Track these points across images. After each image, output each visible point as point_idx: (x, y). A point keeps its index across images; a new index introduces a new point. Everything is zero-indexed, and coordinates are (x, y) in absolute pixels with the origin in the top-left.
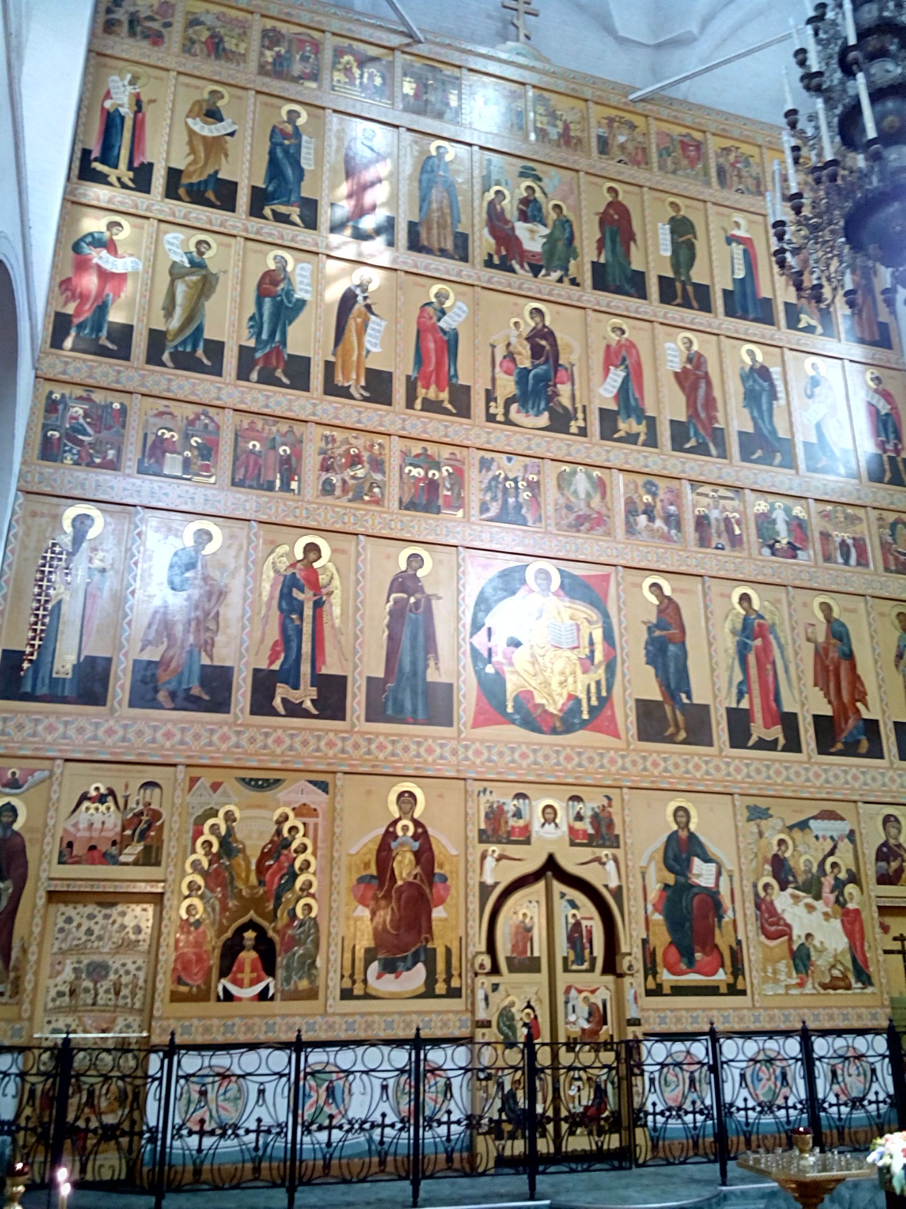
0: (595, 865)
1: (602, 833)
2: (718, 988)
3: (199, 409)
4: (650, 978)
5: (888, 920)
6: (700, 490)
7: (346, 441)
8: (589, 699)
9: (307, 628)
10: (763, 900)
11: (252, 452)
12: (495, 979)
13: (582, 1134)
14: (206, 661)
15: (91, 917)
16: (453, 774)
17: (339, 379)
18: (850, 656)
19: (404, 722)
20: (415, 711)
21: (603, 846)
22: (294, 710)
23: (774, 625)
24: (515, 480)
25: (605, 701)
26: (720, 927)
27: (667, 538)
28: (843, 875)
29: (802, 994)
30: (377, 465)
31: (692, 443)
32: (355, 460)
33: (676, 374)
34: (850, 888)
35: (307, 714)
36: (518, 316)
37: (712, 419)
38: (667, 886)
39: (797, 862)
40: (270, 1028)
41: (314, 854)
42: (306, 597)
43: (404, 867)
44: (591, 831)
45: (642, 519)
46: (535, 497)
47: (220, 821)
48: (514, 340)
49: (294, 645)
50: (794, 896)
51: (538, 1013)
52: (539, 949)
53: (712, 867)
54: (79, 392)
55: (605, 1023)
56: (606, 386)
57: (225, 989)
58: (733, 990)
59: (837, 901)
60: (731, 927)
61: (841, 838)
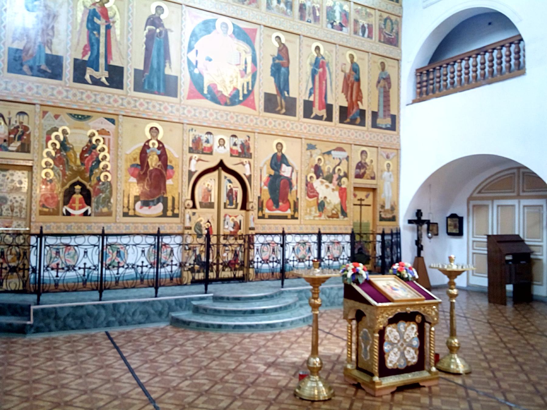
0: (241, 165)
1: (245, 152)
5: (357, 193)
8: (243, 90)
9: (102, 40)
12: (194, 210)
16: (177, 121)
18: (358, 80)
20: (159, 87)
21: (245, 157)
22: (96, 82)
23: (328, 63)
25: (250, 92)
27: (285, 13)
28: (342, 174)
34: (344, 179)
35: (103, 85)
38: (270, 175)
41: (109, 152)
42: (101, 22)
43: (153, 161)
44: (240, 151)
47: (60, 133)
49: (95, 47)
50: (322, 182)
51: (212, 224)
52: (214, 199)
53: (290, 169)
55: (240, 229)
57: (66, 210)
58: (293, 217)
59: (338, 184)
61: (343, 159)
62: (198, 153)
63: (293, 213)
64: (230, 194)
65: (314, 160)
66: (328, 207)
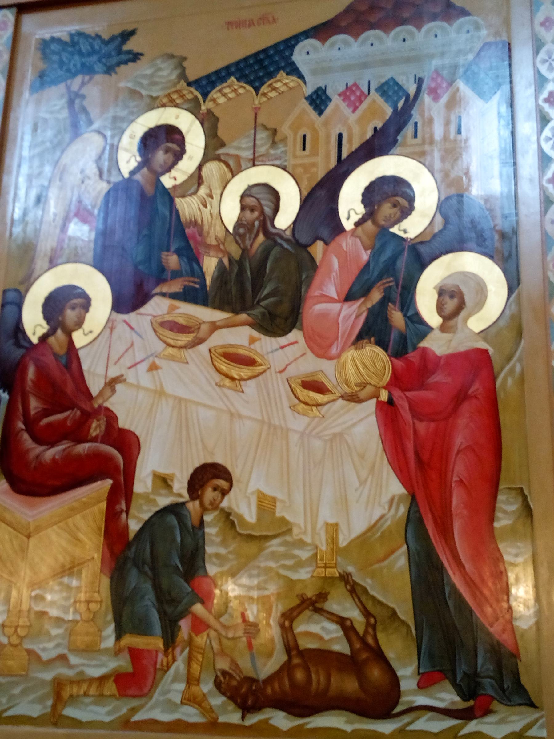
29: (126, 724)
66: (240, 593)
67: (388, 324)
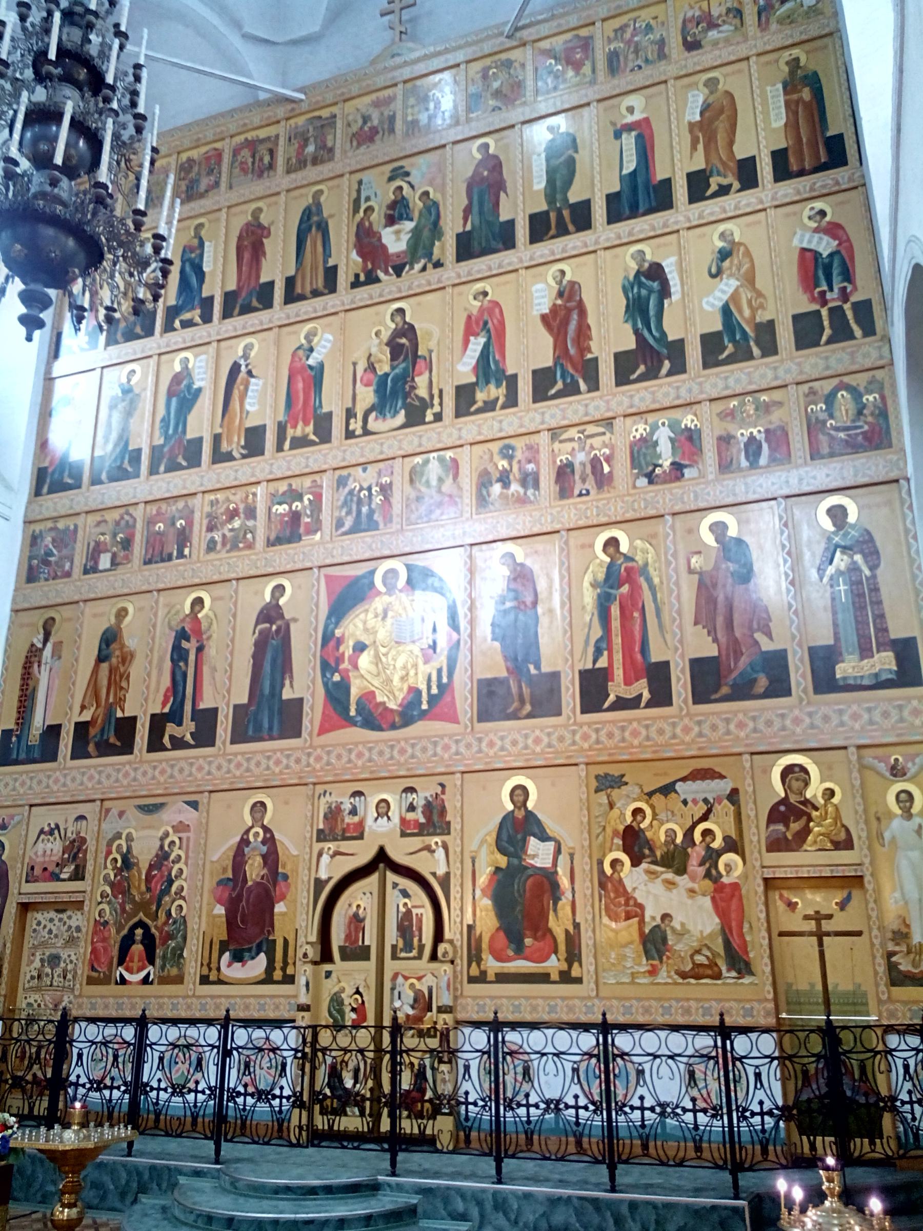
0: (425, 853)
1: (434, 820)
2: (548, 975)
3: (122, 510)
4: (474, 964)
6: (564, 437)
7: (228, 500)
8: (429, 688)
10: (609, 878)
11: (159, 533)
12: (327, 967)
13: (354, 1115)
14: (119, 714)
15: (51, 920)
17: (225, 447)
19: (261, 739)
20: (271, 728)
22: (178, 744)
24: (369, 489)
26: (555, 910)
27: (522, 501)
28: (717, 844)
29: (653, 984)
30: (251, 513)
31: (559, 385)
32: (233, 514)
33: (544, 318)
35: (187, 746)
36: (380, 324)
37: (583, 349)
38: (498, 869)
39: (657, 833)
40: (553, 1009)
41: (186, 864)
42: (190, 646)
43: (254, 870)
44: (422, 820)
45: (497, 488)
46: (387, 499)
47: (123, 842)
48: (374, 350)
50: (648, 872)
52: (370, 938)
53: (551, 845)
54: (50, 524)
55: (430, 1010)
56: (465, 359)
58: (566, 978)
59: (708, 875)
60: (568, 909)
61: (719, 800)
62: (335, 840)
63: (565, 967)
64: (406, 926)
65: (623, 815)
67: (712, 875)
